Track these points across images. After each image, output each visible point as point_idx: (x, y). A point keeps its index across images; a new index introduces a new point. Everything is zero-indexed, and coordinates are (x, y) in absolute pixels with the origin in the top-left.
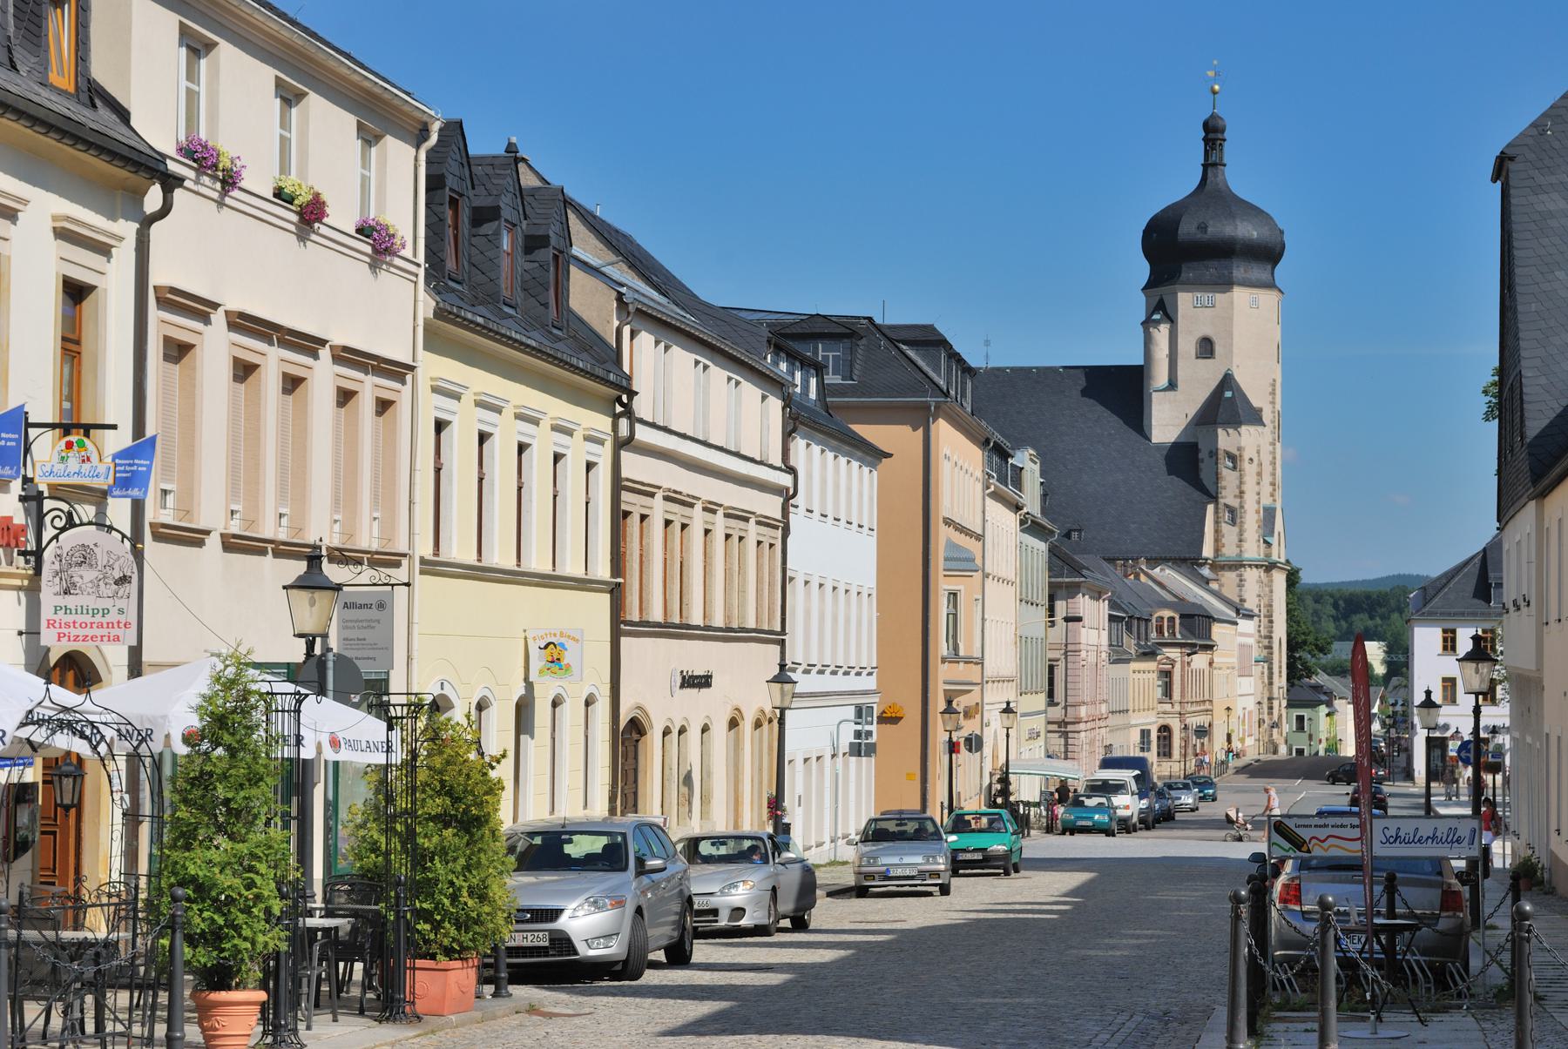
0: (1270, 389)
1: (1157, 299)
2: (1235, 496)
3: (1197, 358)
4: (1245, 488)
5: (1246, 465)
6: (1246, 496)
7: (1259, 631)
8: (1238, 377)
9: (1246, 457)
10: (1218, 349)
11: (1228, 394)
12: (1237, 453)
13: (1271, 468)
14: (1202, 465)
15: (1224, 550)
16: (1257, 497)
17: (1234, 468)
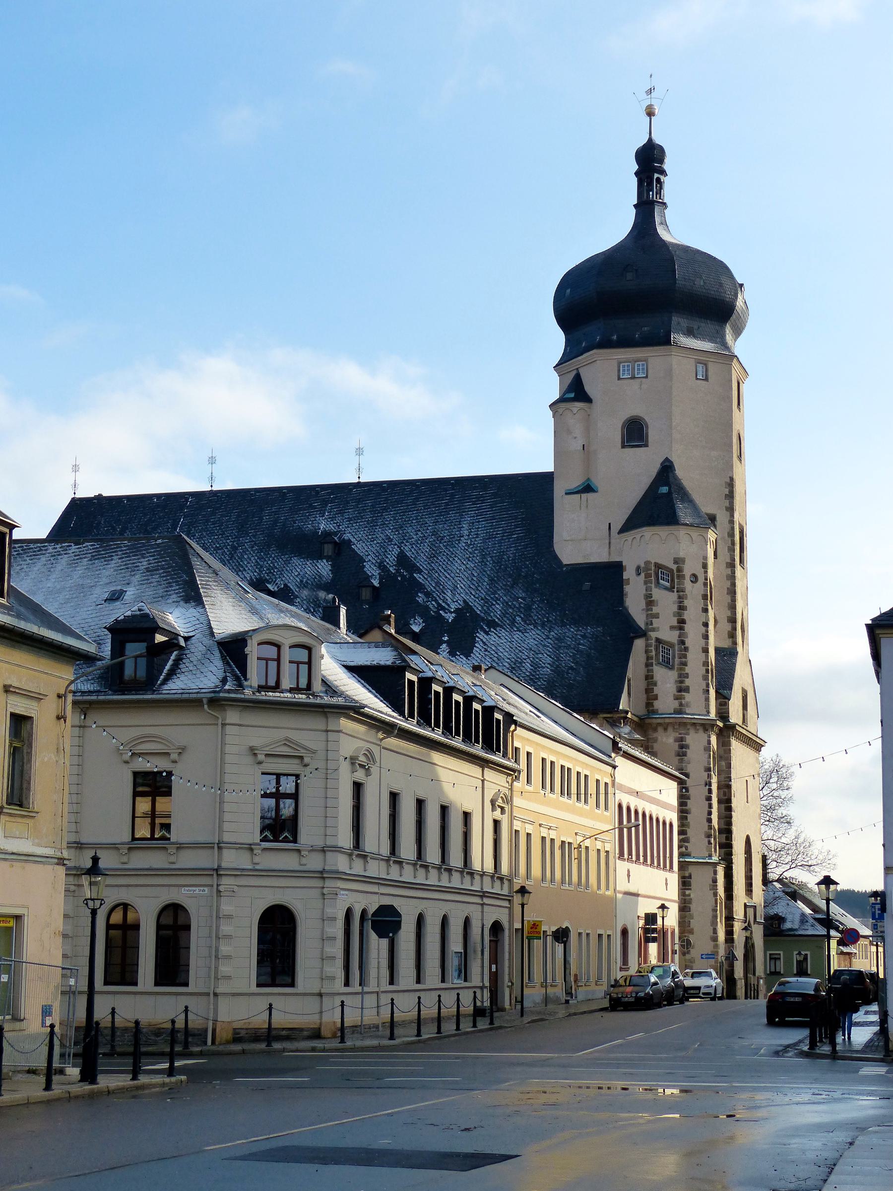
0: (727, 491)
1: (574, 373)
2: (672, 628)
3: (623, 446)
4: (686, 615)
5: (687, 584)
6: (687, 627)
7: (710, 821)
8: (679, 472)
9: (687, 572)
10: (653, 434)
11: (664, 490)
12: (674, 567)
13: (728, 599)
14: (627, 589)
15: (657, 705)
16: (704, 629)
17: (671, 589)
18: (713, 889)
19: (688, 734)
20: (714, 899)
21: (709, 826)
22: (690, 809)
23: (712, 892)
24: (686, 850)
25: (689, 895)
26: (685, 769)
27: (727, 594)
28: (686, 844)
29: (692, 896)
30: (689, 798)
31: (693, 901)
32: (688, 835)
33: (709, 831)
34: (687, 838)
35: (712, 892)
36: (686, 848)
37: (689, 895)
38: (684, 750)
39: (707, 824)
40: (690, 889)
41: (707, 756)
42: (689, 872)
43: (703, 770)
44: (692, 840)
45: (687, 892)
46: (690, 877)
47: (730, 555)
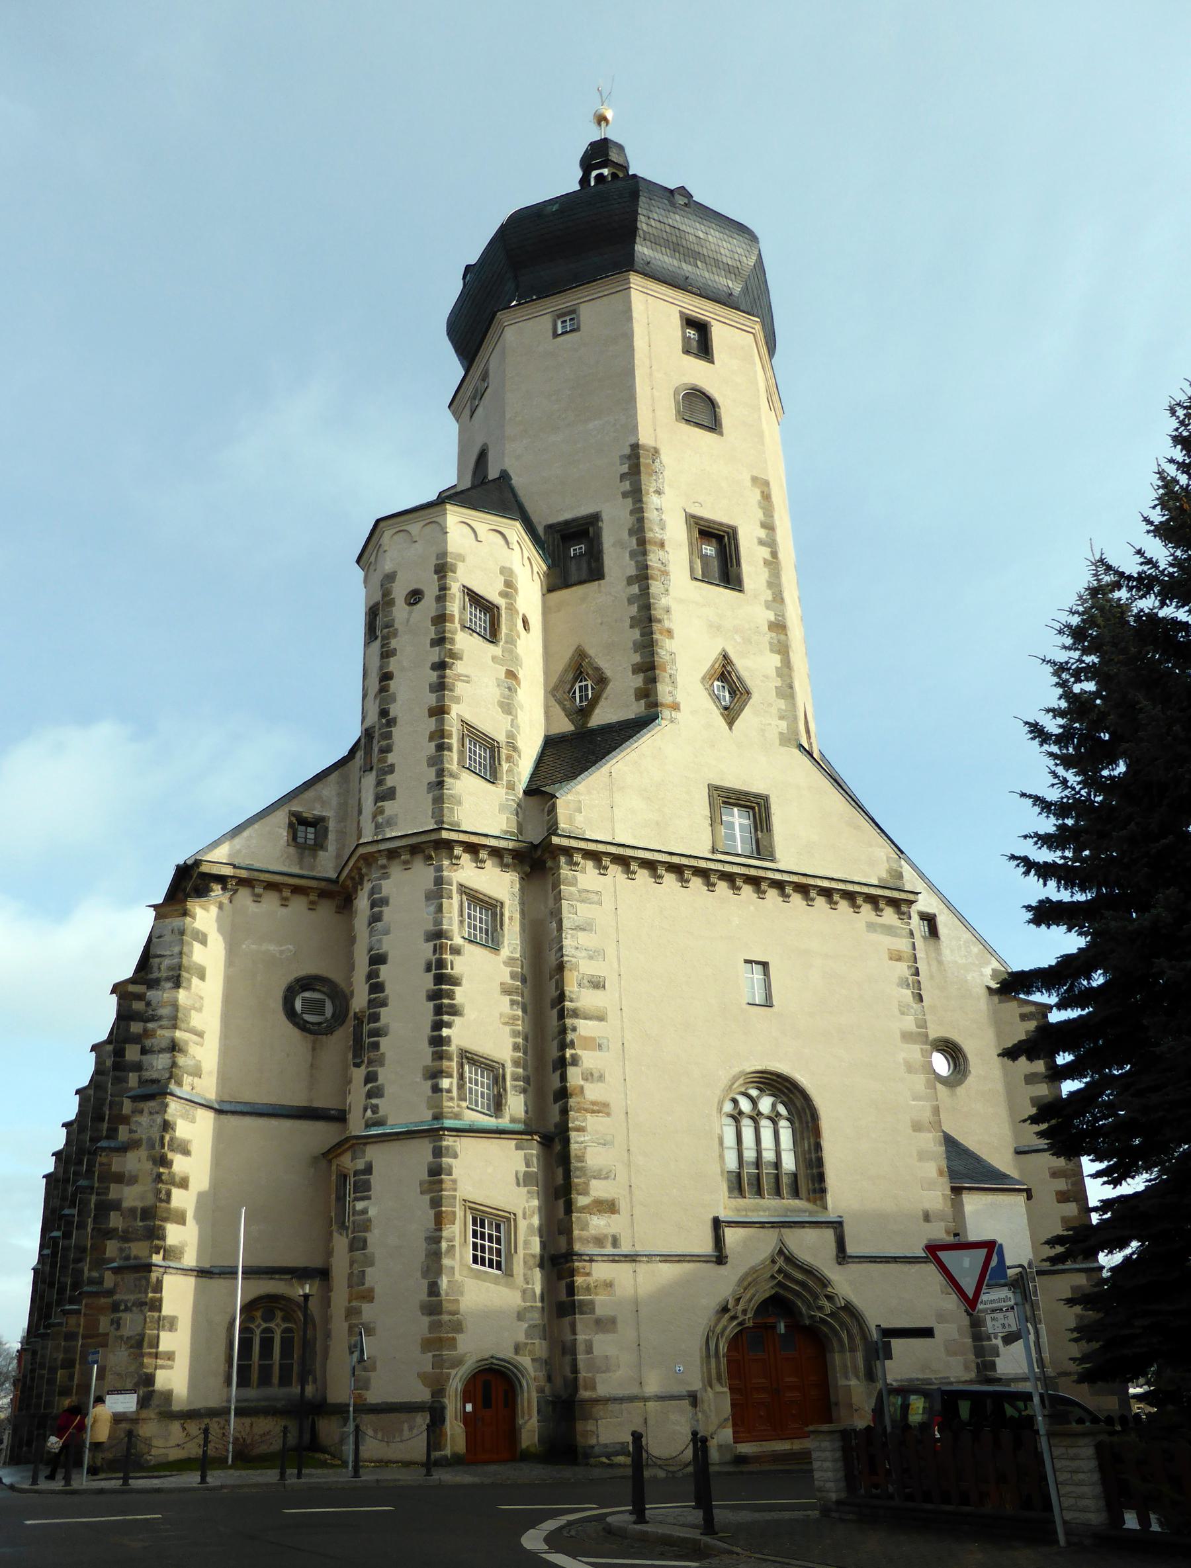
18: (430, 1191)
19: (386, 876)
20: (432, 1213)
21: (434, 1053)
22: (387, 1026)
23: (427, 1197)
24: (374, 1112)
25: (364, 1211)
26: (376, 947)
27: (632, 627)
28: (374, 1101)
29: (372, 1212)
30: (384, 1004)
31: (374, 1222)
32: (380, 1082)
33: (437, 1063)
34: (377, 1087)
35: (427, 1197)
36: (375, 1109)
37: (364, 1211)
38: (376, 909)
39: (428, 1051)
40: (369, 1198)
41: (432, 909)
42: (367, 1159)
43: (421, 937)
44: (388, 1091)
45: (360, 1206)
46: (368, 1170)
47: (637, 562)
